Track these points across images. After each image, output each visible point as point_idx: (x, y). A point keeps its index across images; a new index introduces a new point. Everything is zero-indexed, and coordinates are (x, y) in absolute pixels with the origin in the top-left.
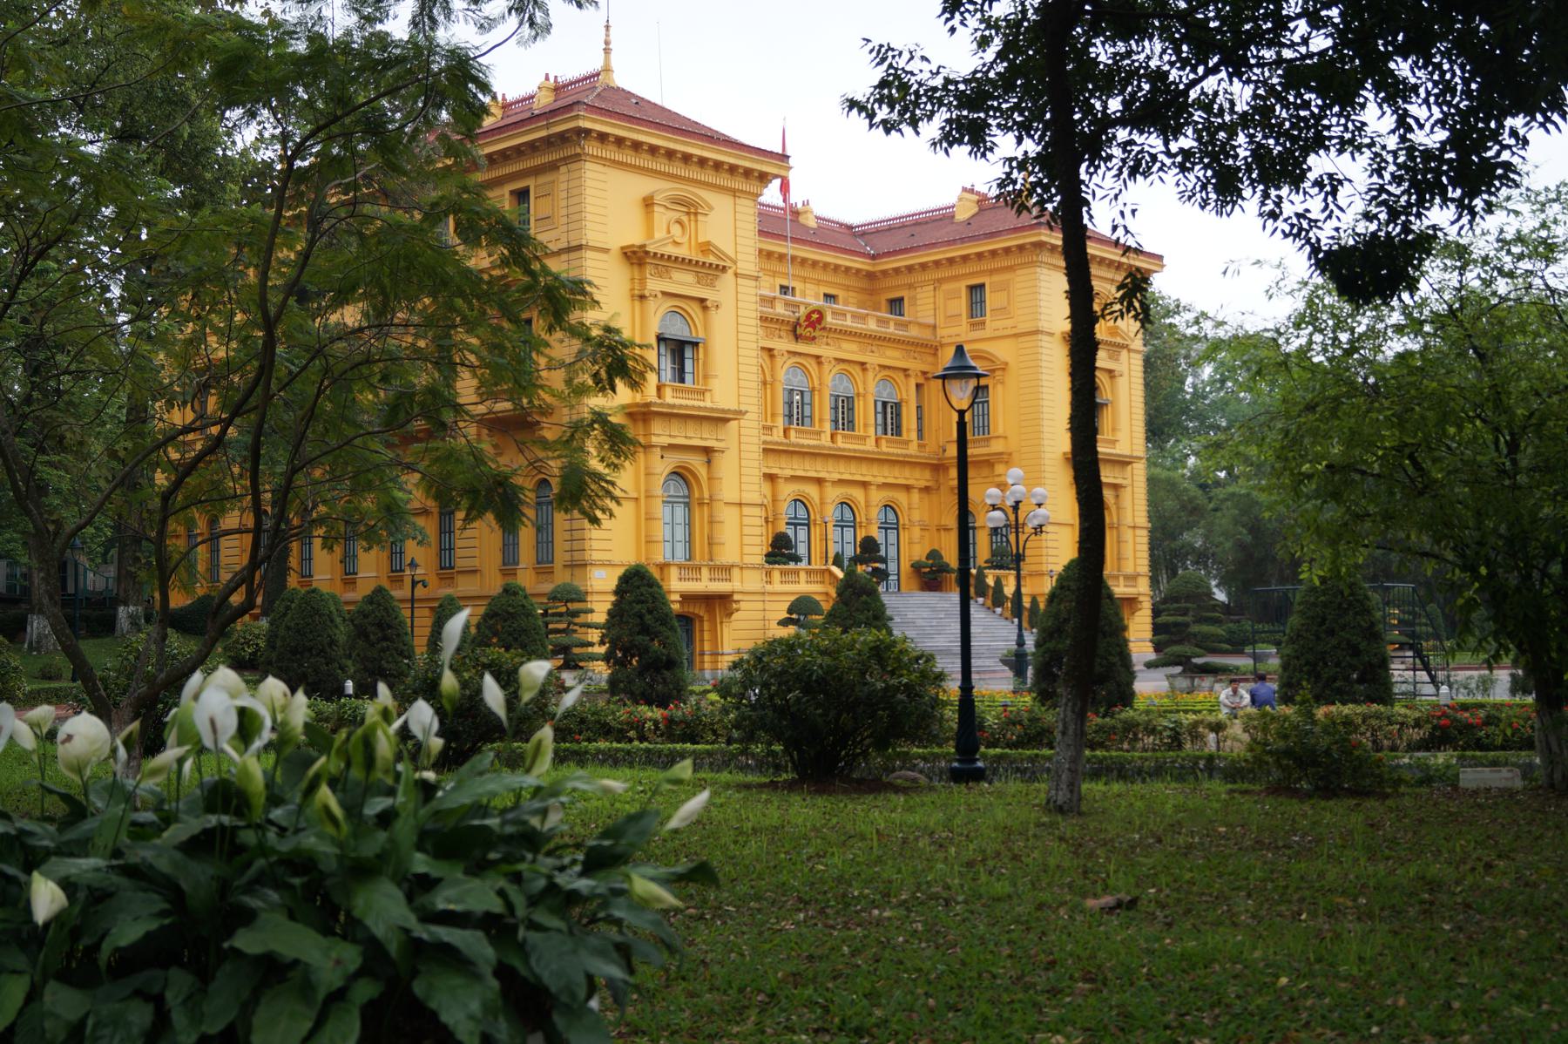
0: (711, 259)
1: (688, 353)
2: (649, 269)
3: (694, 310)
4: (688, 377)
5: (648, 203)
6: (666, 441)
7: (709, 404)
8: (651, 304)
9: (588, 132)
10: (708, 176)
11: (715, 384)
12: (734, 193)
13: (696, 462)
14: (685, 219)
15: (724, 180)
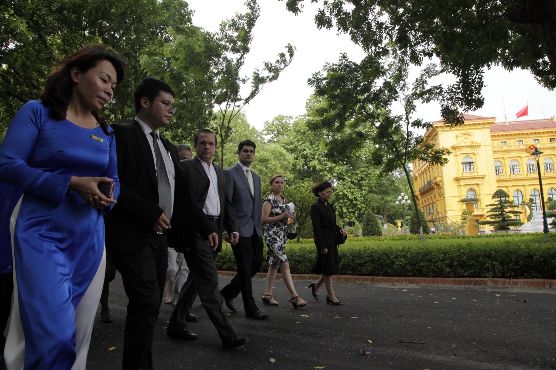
0: (474, 144)
1: (472, 164)
2: (457, 150)
3: (472, 155)
4: (472, 170)
5: (457, 137)
6: (464, 184)
7: (476, 174)
8: (458, 156)
9: (437, 127)
10: (474, 127)
11: (479, 171)
12: (482, 128)
13: (475, 187)
14: (467, 137)
15: (478, 127)
